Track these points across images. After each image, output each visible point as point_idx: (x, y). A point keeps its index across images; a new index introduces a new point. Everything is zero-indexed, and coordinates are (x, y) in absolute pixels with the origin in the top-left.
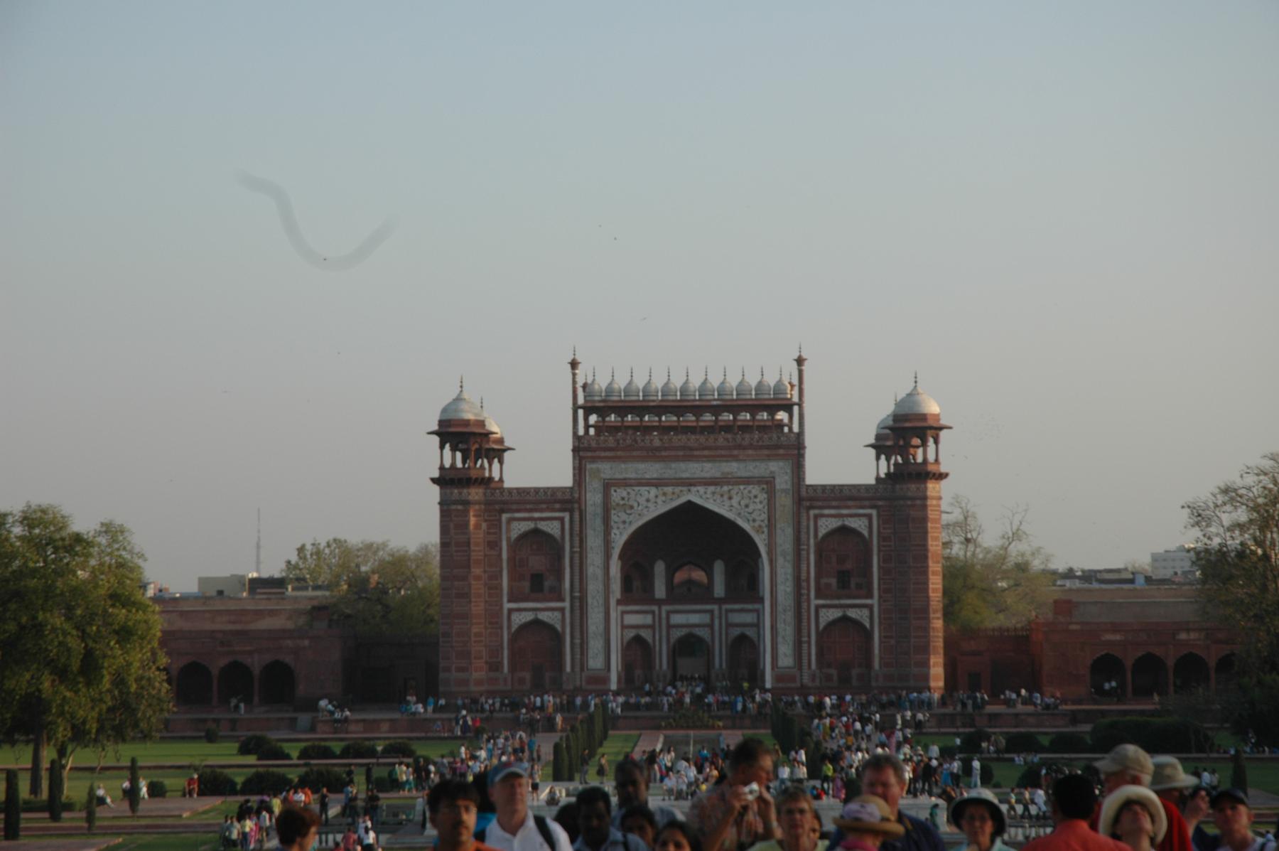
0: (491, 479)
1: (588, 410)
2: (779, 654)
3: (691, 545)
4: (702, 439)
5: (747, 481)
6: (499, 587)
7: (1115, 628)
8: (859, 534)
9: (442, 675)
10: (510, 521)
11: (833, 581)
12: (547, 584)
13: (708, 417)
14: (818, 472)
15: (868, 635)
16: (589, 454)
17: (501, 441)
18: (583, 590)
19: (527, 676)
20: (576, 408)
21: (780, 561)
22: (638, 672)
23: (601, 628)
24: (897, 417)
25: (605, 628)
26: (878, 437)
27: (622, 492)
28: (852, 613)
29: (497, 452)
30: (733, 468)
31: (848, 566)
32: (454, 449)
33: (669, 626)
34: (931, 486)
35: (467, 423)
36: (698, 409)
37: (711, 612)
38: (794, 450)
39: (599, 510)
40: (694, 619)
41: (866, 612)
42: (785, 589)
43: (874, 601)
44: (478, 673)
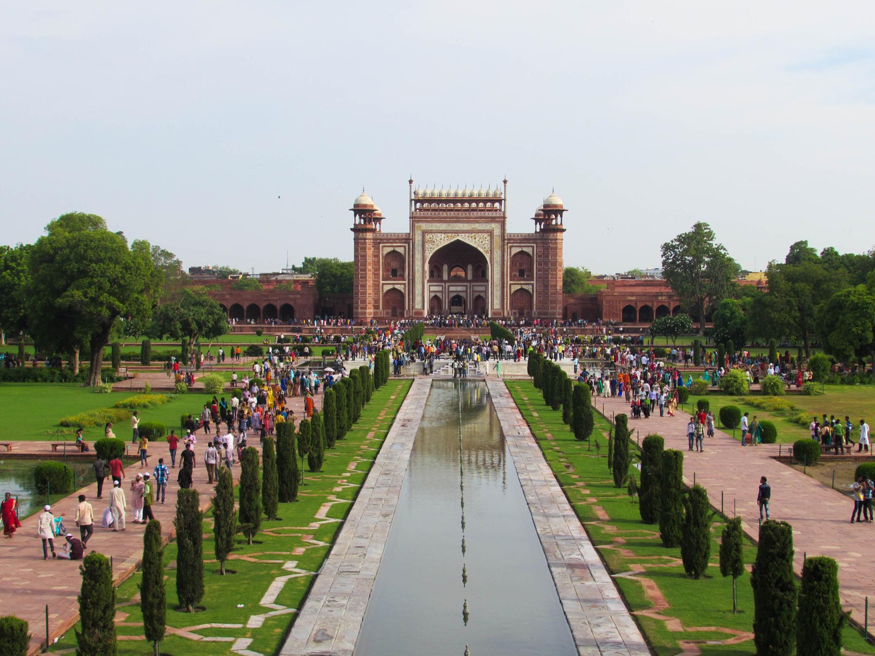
0: (375, 230)
1: (416, 201)
2: (494, 303)
3: (459, 258)
4: (464, 213)
5: (482, 232)
6: (378, 274)
7: (632, 294)
8: (528, 254)
9: (355, 310)
10: (383, 247)
11: (518, 274)
12: (398, 273)
13: (467, 205)
14: (510, 229)
15: (531, 296)
17: (380, 215)
18: (413, 276)
19: (390, 311)
20: (411, 200)
21: (495, 265)
22: (436, 311)
23: (421, 292)
24: (545, 206)
25: (422, 293)
26: (536, 215)
27: (430, 236)
28: (525, 287)
29: (378, 220)
30: (477, 226)
31: (524, 267)
32: (361, 218)
33: (449, 292)
34: (559, 235)
35: (366, 206)
36: (462, 201)
38: (502, 221)
39: (420, 243)
40: (459, 289)
41: (531, 287)
42: (497, 276)
43: (534, 282)
44: (370, 311)
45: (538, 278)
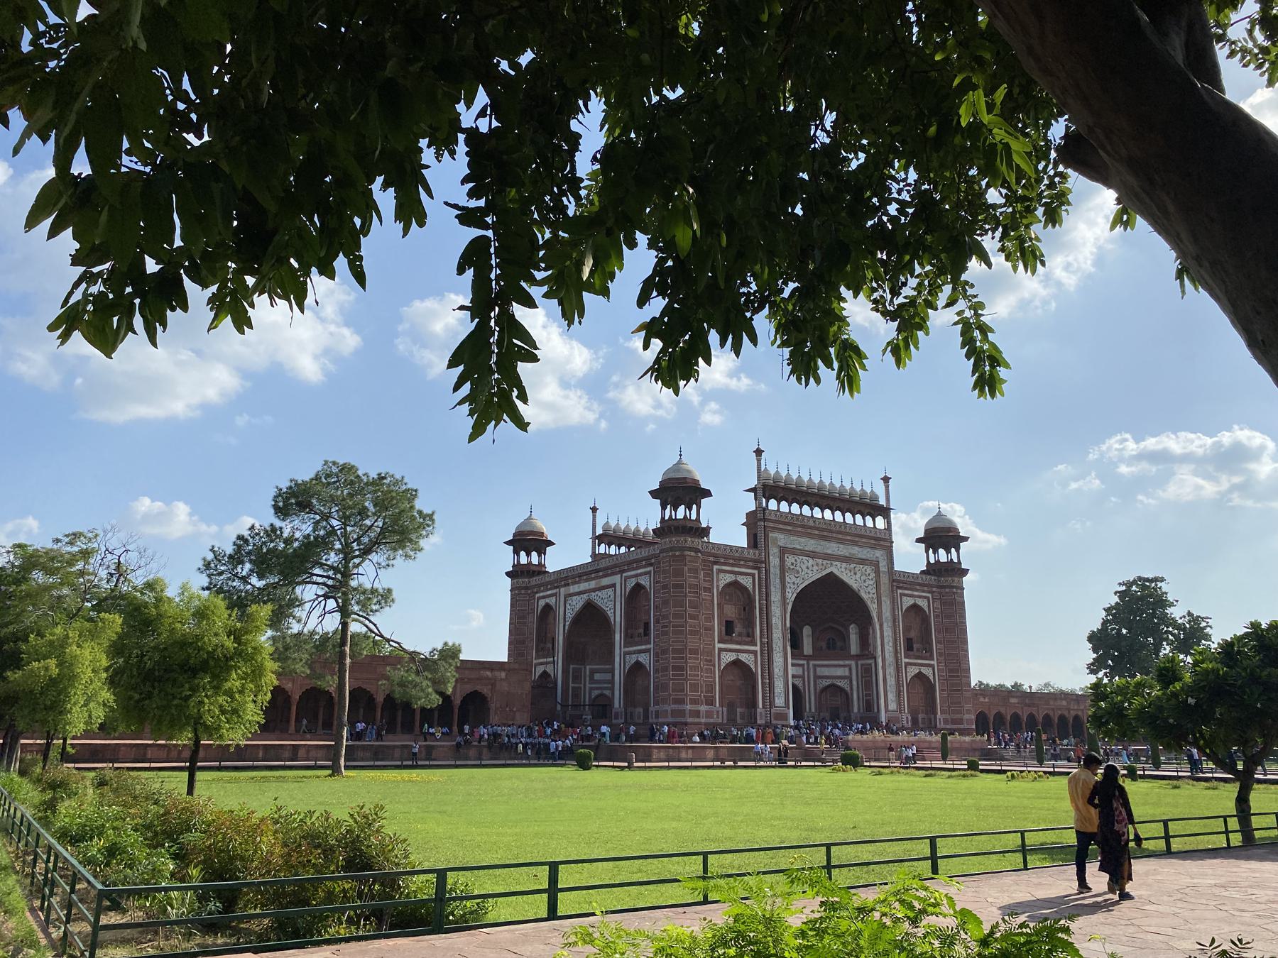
5: (863, 561)
10: (719, 571)
15: (932, 687)
16: (771, 525)
21: (885, 625)
30: (856, 551)
31: (913, 634)
37: (802, 665)
39: (778, 571)
42: (889, 648)
43: (934, 662)
45: (939, 654)
